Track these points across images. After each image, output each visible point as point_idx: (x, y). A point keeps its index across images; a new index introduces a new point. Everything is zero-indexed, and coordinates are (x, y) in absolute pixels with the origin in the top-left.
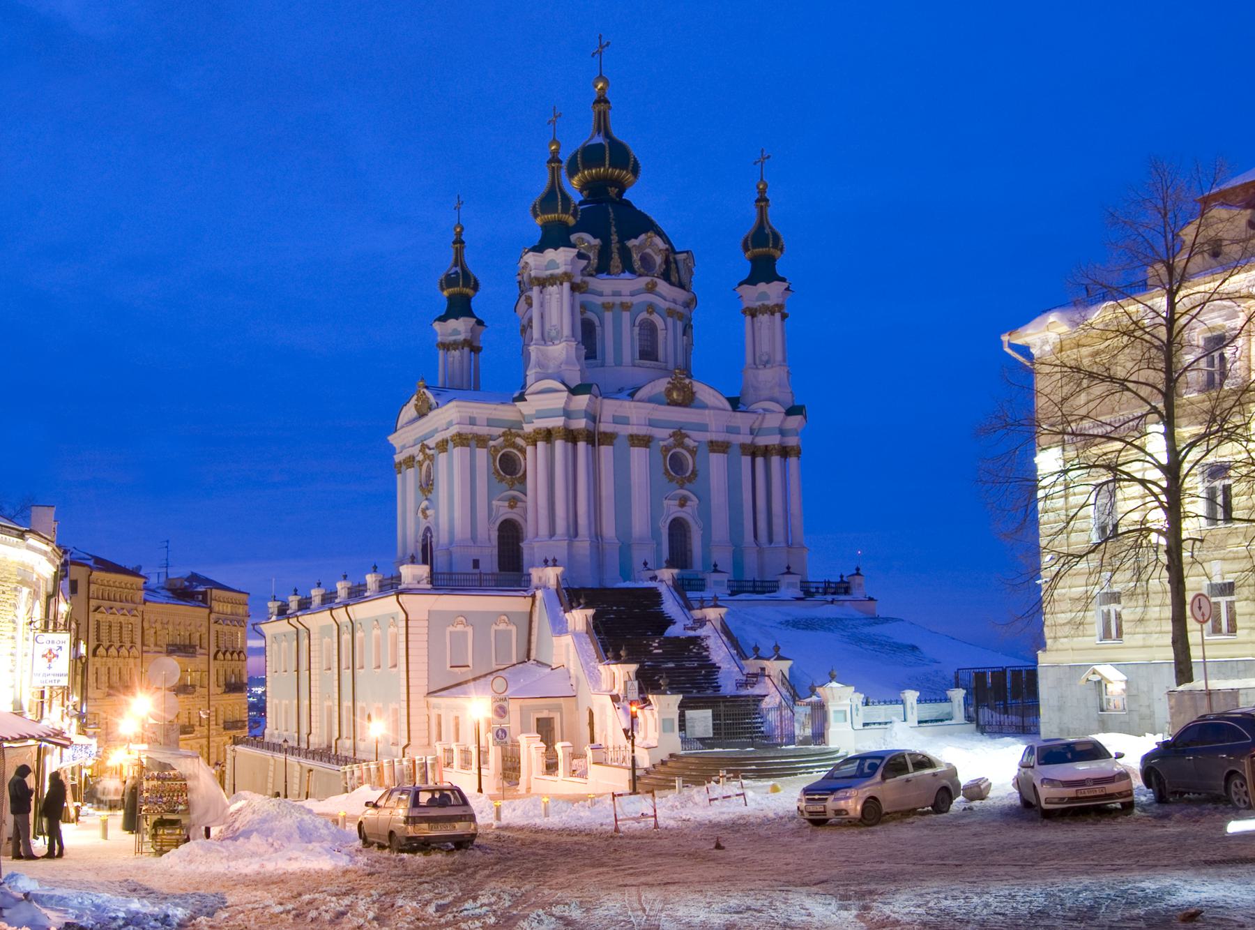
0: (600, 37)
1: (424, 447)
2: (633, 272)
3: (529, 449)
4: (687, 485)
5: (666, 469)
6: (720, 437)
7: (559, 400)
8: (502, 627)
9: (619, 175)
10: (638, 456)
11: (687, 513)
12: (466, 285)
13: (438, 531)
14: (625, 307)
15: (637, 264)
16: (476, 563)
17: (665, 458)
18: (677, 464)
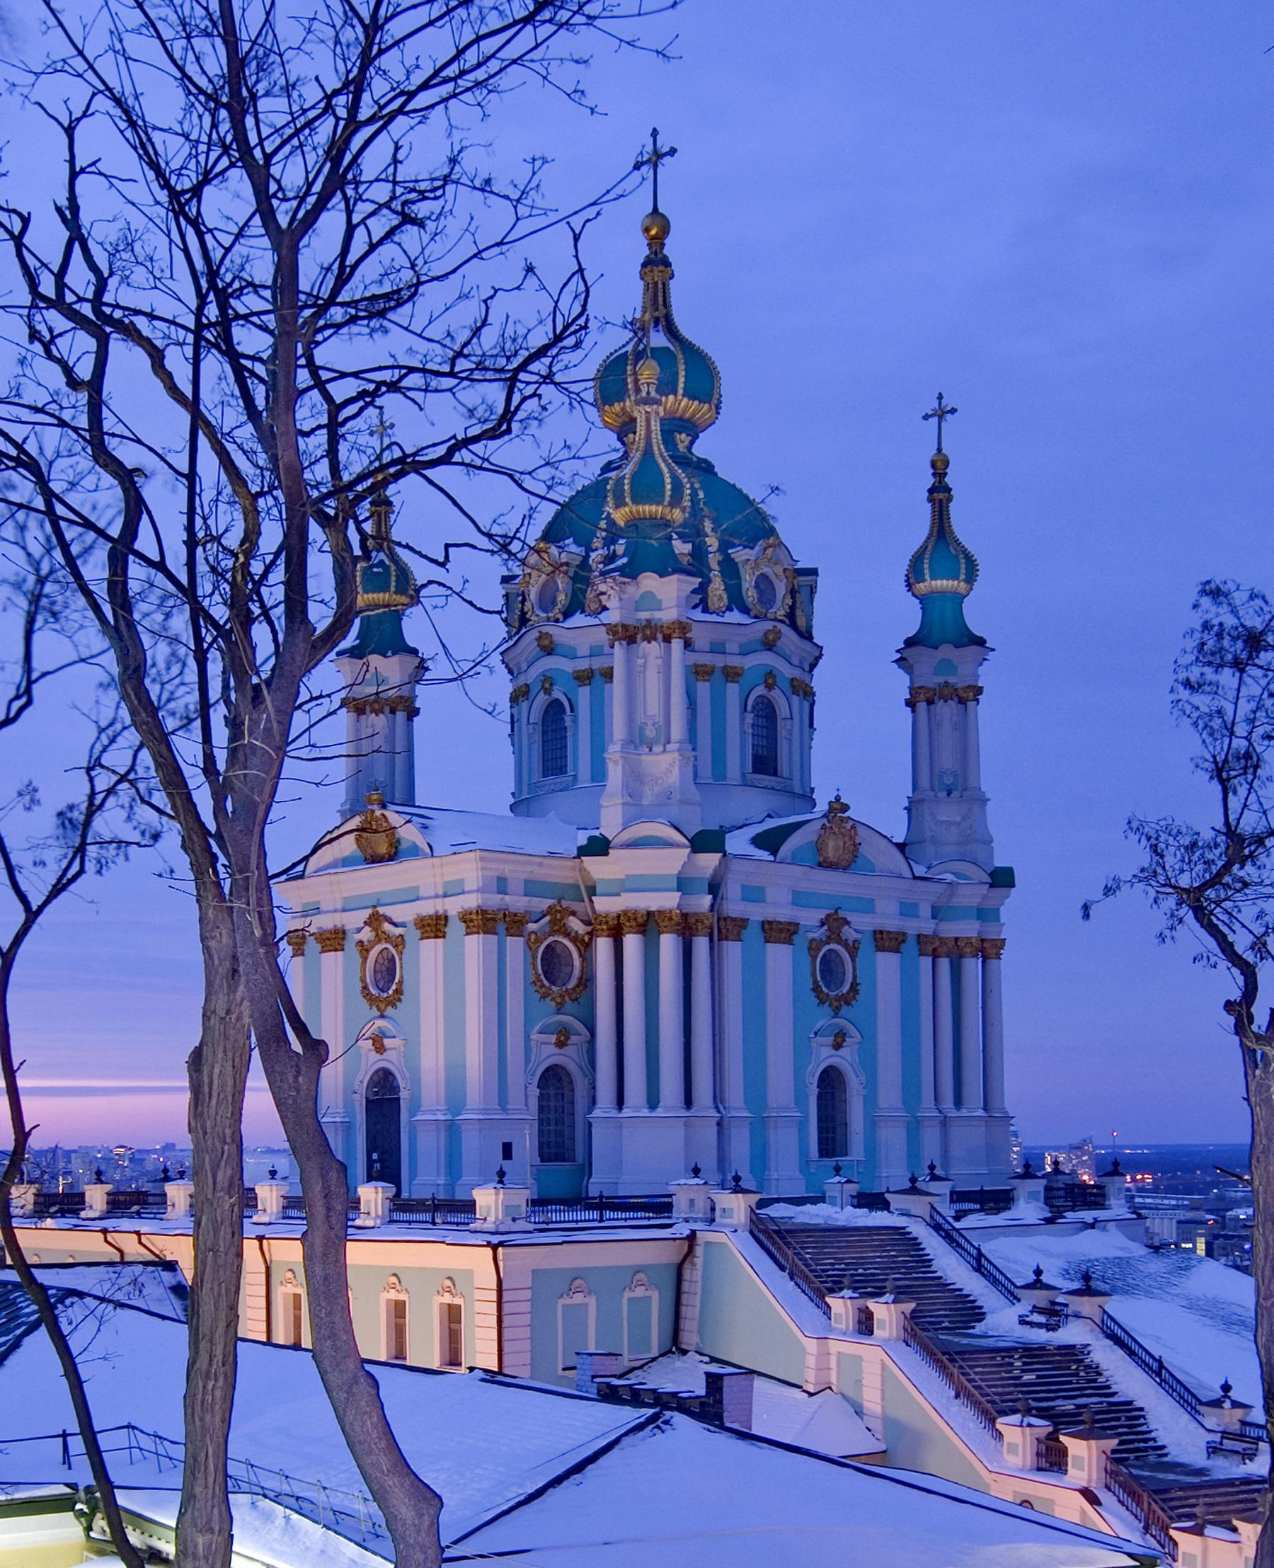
0: (655, 133)
1: (375, 920)
2: (745, 610)
3: (603, 946)
4: (845, 1010)
5: (815, 982)
6: (892, 923)
7: (673, 860)
8: (640, 1292)
10: (779, 958)
11: (845, 1059)
12: (401, 590)
13: (416, 1082)
14: (732, 674)
15: (750, 595)
16: (507, 1151)
17: (814, 962)
18: (830, 969)
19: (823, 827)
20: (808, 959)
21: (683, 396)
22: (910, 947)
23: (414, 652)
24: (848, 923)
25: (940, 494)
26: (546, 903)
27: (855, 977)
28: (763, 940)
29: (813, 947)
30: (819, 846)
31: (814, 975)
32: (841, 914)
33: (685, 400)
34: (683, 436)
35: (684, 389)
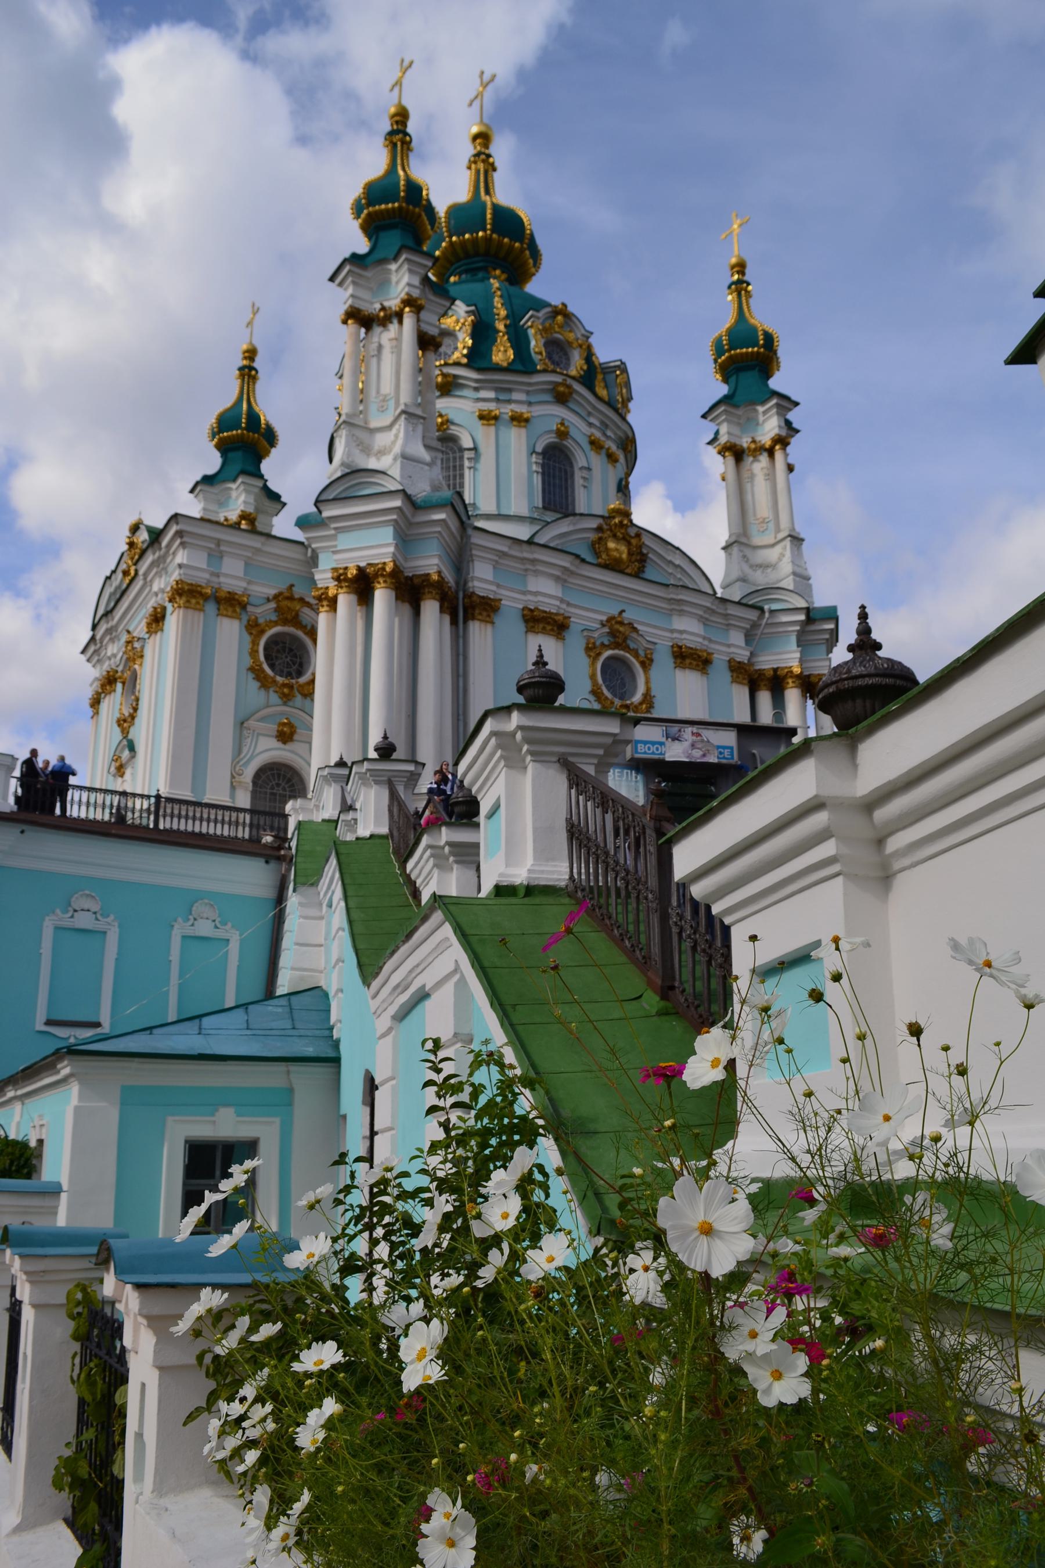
8: (204, 928)
9: (511, 248)
19: (599, 529)
21: (493, 231)
23: (261, 477)
24: (635, 630)
25: (740, 287)
26: (272, 592)
27: (648, 689)
28: (525, 629)
29: (592, 650)
30: (597, 546)
31: (593, 677)
32: (628, 616)
33: (494, 236)
34: (498, 272)
35: (493, 224)
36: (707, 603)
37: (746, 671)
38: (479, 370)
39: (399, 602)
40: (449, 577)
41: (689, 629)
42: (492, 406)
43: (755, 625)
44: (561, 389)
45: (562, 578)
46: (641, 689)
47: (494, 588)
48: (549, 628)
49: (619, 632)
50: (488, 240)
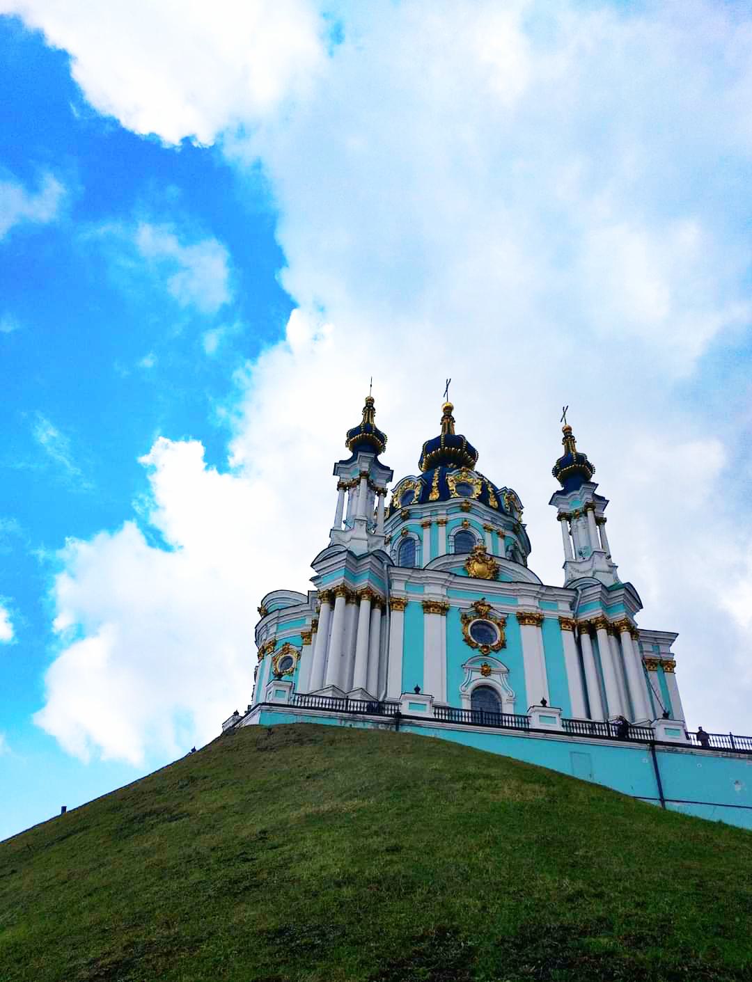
19: (469, 559)
20: (463, 625)
22: (551, 625)
24: (492, 608)
29: (465, 619)
36: (537, 589)
37: (571, 623)
38: (422, 503)
39: (350, 605)
40: (378, 591)
41: (528, 604)
42: (427, 519)
43: (575, 599)
44: (465, 505)
45: (447, 585)
46: (499, 638)
47: (404, 594)
48: (436, 610)
49: (480, 608)
50: (442, 451)
